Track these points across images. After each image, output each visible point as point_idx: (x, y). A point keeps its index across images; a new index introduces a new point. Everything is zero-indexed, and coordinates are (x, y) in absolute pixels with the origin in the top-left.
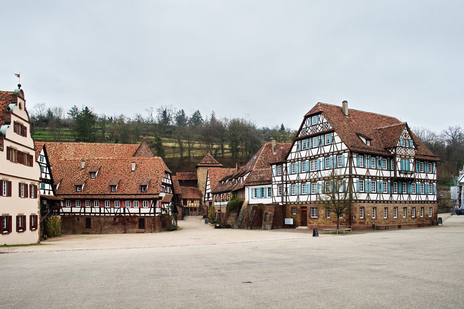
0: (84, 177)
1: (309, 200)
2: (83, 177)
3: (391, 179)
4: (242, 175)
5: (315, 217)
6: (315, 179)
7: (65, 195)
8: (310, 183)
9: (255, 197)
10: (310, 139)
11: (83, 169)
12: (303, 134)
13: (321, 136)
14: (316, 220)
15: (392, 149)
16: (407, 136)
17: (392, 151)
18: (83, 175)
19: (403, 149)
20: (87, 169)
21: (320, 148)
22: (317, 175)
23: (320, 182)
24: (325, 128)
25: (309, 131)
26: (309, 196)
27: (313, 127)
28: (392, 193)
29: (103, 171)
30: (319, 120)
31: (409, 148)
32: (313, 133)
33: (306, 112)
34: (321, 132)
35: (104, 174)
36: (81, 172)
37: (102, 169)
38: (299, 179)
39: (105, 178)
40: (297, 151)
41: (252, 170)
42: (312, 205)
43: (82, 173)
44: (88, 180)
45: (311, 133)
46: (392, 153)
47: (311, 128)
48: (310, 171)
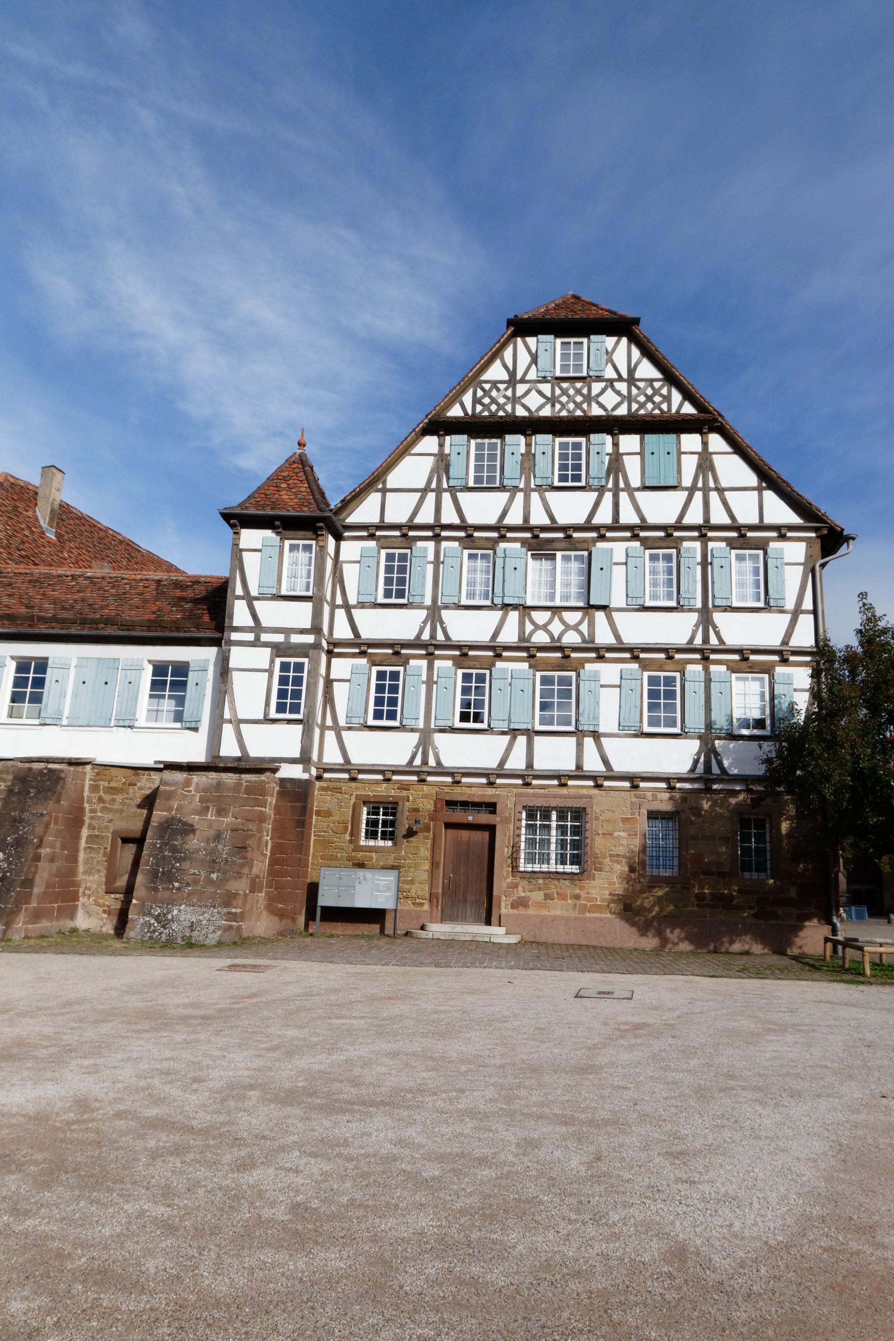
33: (526, 310)
40: (434, 486)
42: (534, 795)
47: (546, 388)
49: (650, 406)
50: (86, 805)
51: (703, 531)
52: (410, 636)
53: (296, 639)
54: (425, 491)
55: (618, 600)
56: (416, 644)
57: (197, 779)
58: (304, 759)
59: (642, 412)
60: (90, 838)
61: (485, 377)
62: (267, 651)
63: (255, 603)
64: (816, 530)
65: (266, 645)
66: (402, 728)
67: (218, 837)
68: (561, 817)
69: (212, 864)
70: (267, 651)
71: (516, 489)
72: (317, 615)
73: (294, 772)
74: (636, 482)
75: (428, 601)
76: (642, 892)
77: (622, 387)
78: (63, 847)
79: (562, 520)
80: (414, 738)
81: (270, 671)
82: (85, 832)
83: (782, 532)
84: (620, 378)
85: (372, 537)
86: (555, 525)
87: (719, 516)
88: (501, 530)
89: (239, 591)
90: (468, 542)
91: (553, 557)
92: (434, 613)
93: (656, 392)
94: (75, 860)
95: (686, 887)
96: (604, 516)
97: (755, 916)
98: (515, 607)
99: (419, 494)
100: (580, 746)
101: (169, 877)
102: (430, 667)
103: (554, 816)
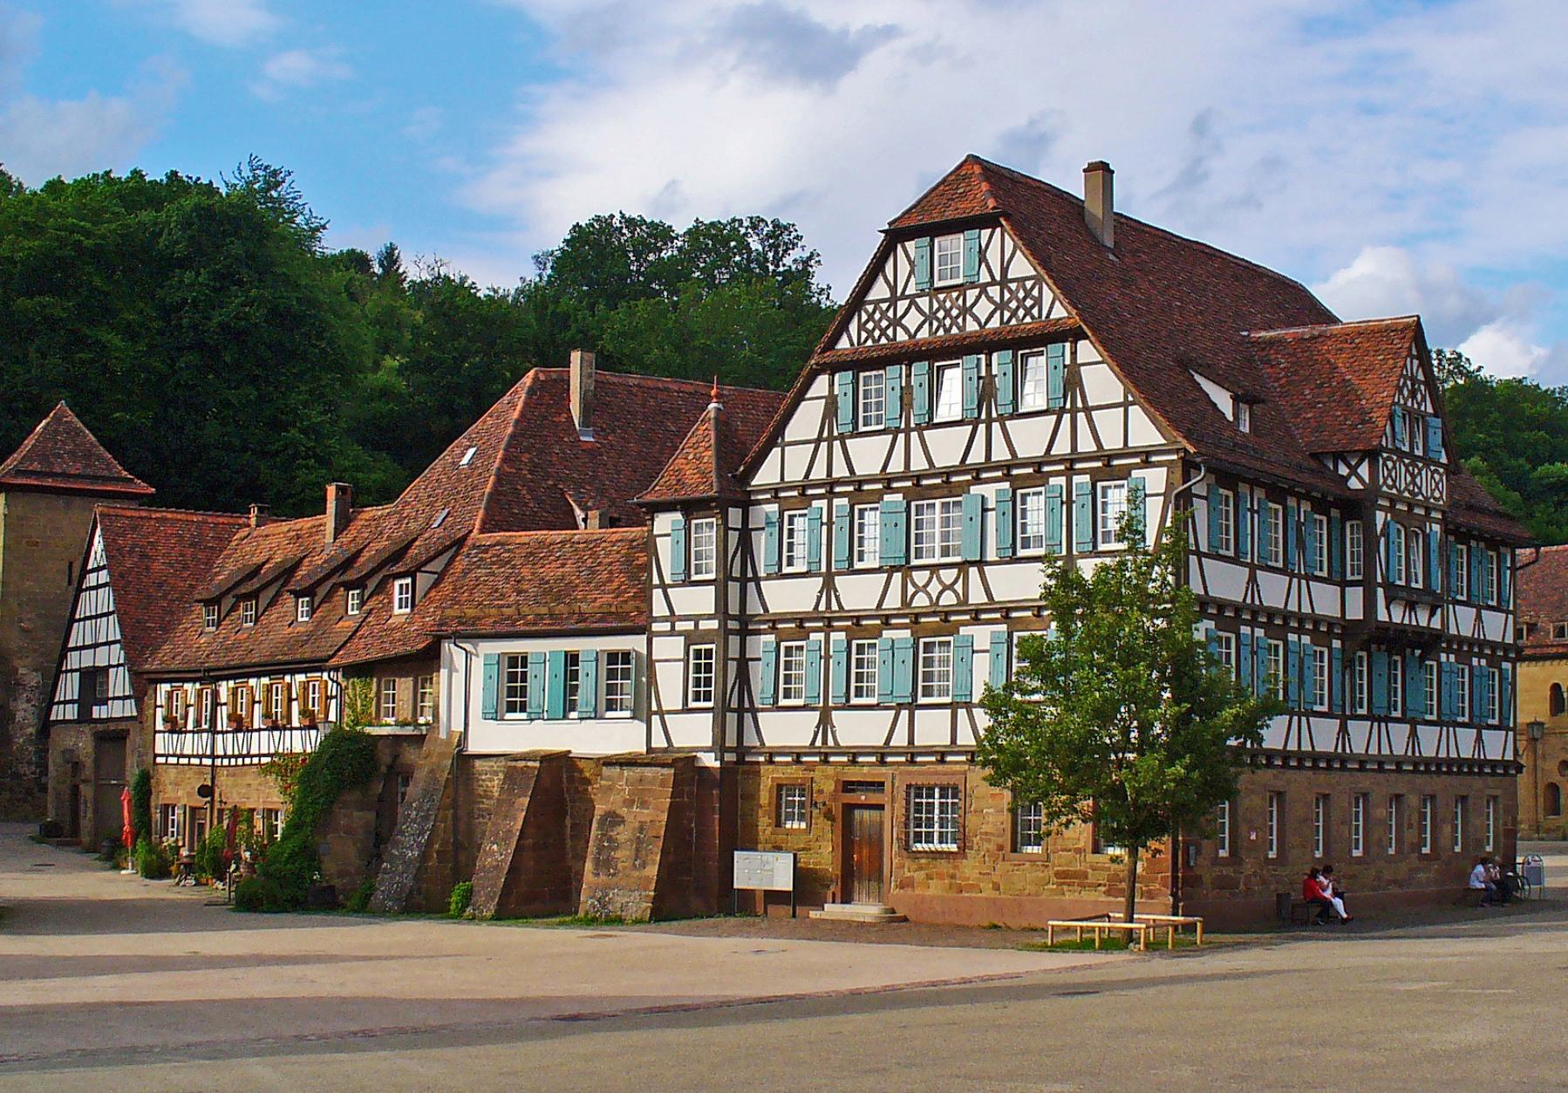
1: (900, 739)
3: (1347, 629)
6: (947, 614)
8: (907, 633)
10: (920, 368)
12: (870, 333)
13: (995, 356)
14: (943, 866)
15: (1353, 463)
16: (1419, 397)
17: (1353, 471)
19: (1404, 465)
21: (982, 427)
22: (959, 587)
24: (1021, 313)
25: (912, 321)
26: (905, 714)
27: (941, 296)
28: (1348, 713)
30: (982, 258)
31: (1428, 461)
32: (941, 332)
33: (893, 211)
34: (995, 331)
38: (835, 607)
40: (825, 434)
41: (465, 537)
45: (924, 334)
46: (1354, 484)
47: (923, 302)
48: (914, 562)
50: (566, 796)
53: (705, 625)
54: (818, 441)
56: (814, 616)
58: (719, 747)
61: (870, 297)
63: (669, 590)
65: (680, 634)
66: (804, 708)
71: (897, 431)
75: (824, 569)
77: (994, 291)
79: (939, 463)
80: (815, 716)
83: (1146, 457)
84: (993, 283)
86: (933, 471)
87: (1086, 445)
89: (656, 581)
96: (977, 456)
99: (813, 446)
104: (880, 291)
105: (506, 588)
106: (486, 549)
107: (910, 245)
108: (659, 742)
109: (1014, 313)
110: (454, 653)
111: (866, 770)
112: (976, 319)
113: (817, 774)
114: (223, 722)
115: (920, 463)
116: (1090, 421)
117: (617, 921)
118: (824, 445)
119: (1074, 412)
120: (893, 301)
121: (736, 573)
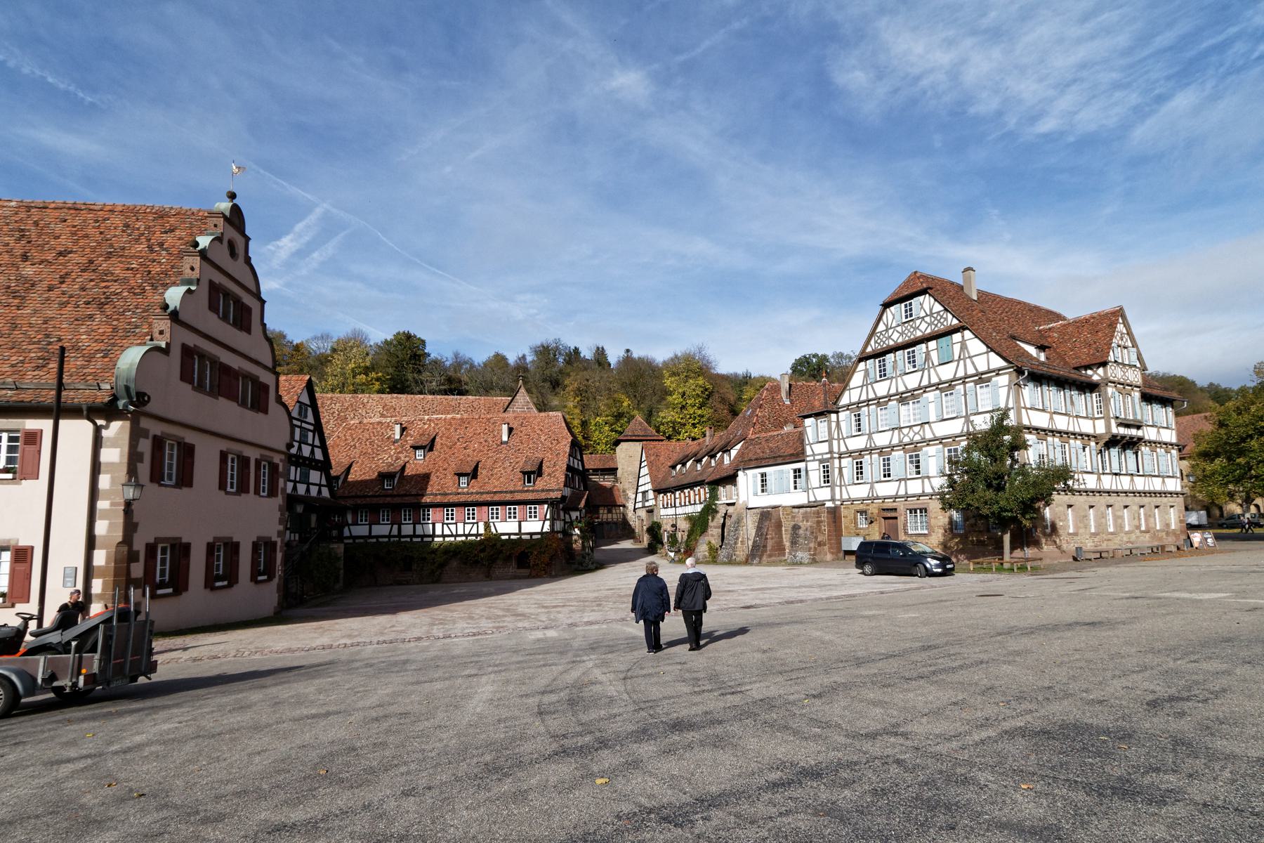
0: (399, 458)
2: (397, 459)
4: (725, 449)
5: (920, 532)
7: (357, 497)
9: (763, 491)
11: (396, 441)
18: (399, 453)
20: (407, 441)
22: (921, 433)
23: (931, 450)
29: (442, 444)
33: (885, 297)
34: (929, 334)
35: (442, 451)
36: (393, 447)
37: (438, 439)
39: (446, 458)
43: (395, 449)
44: (407, 465)
47: (899, 329)
49: (939, 325)
51: (964, 380)
52: (863, 447)
53: (825, 456)
54: (862, 386)
55: (932, 418)
57: (802, 510)
58: (833, 500)
59: (936, 329)
60: (786, 530)
62: (817, 462)
64: (1012, 367)
66: (864, 483)
67: (807, 529)
68: (921, 512)
69: (805, 538)
70: (817, 462)
72: (831, 446)
73: (829, 504)
74: (936, 363)
76: (950, 540)
78: (776, 534)
81: (819, 470)
82: (783, 529)
84: (927, 315)
85: (848, 409)
88: (889, 397)
89: (807, 442)
90: (879, 404)
91: (908, 404)
92: (870, 435)
93: (942, 317)
94: (782, 538)
95: (967, 538)
97: (995, 548)
98: (896, 429)
100: (923, 482)
101: (796, 543)
102: (871, 458)
103: (918, 511)
104: (881, 327)
105: (759, 451)
106: (753, 440)
107: (892, 308)
108: (812, 499)
109: (936, 325)
110: (740, 473)
111: (889, 504)
112: (921, 331)
113: (870, 507)
114: (678, 505)
115: (902, 389)
116: (973, 363)
117: (801, 564)
118: (865, 388)
119: (964, 359)
120: (887, 330)
121: (836, 437)
